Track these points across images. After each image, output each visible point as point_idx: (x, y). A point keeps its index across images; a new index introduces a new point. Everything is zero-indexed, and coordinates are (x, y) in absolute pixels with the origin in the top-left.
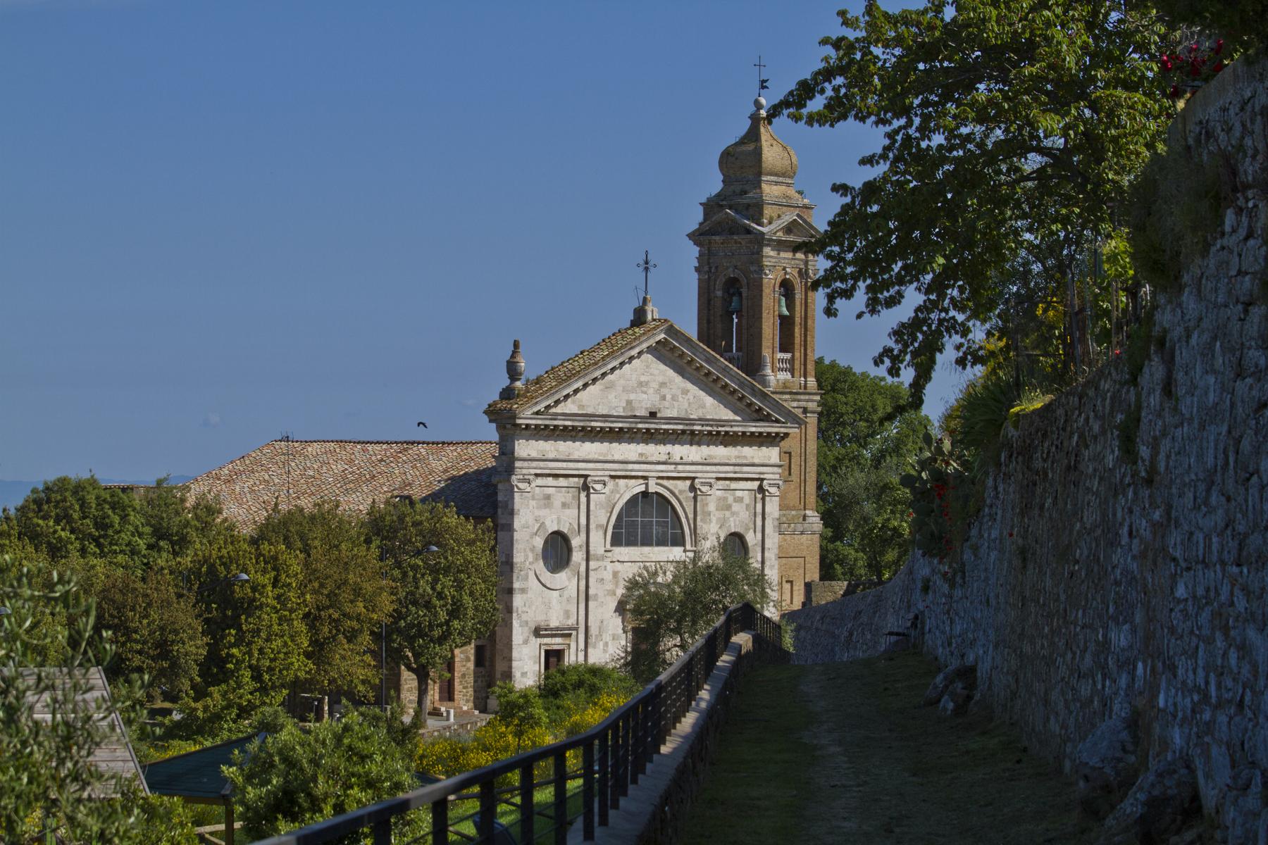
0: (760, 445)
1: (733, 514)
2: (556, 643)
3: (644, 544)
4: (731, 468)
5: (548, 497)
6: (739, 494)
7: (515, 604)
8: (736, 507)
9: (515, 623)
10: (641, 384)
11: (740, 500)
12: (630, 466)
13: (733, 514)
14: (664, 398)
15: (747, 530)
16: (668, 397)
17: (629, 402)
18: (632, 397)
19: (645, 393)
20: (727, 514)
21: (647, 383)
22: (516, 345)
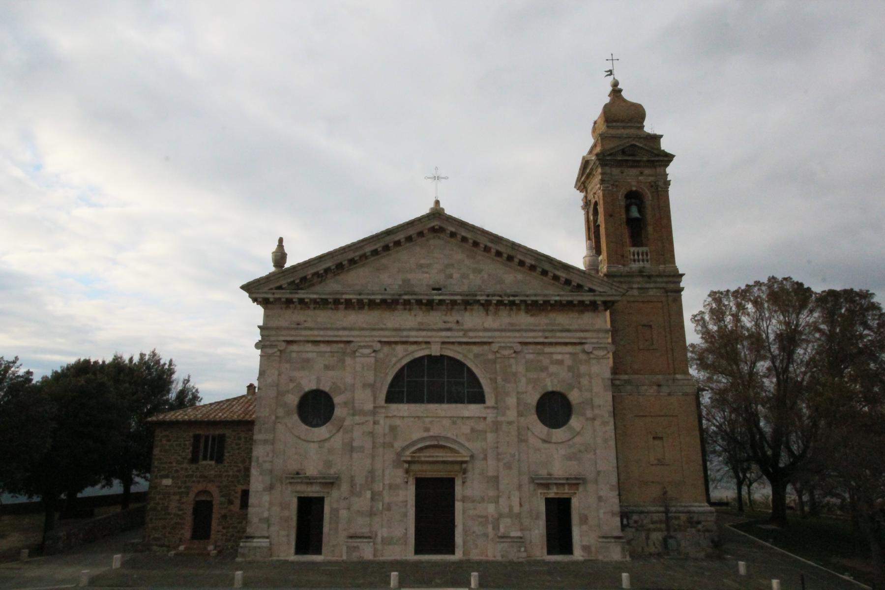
0: (582, 312)
1: (551, 375)
2: (312, 491)
3: (430, 401)
4: (540, 334)
5: (308, 360)
6: (559, 357)
7: (255, 454)
8: (553, 369)
9: (254, 472)
10: (421, 266)
11: (560, 362)
12: (405, 333)
13: (551, 375)
14: (450, 276)
15: (571, 387)
16: (456, 276)
17: (404, 281)
18: (409, 276)
19: (426, 273)
20: (543, 375)
21: (429, 266)
22: (281, 240)
